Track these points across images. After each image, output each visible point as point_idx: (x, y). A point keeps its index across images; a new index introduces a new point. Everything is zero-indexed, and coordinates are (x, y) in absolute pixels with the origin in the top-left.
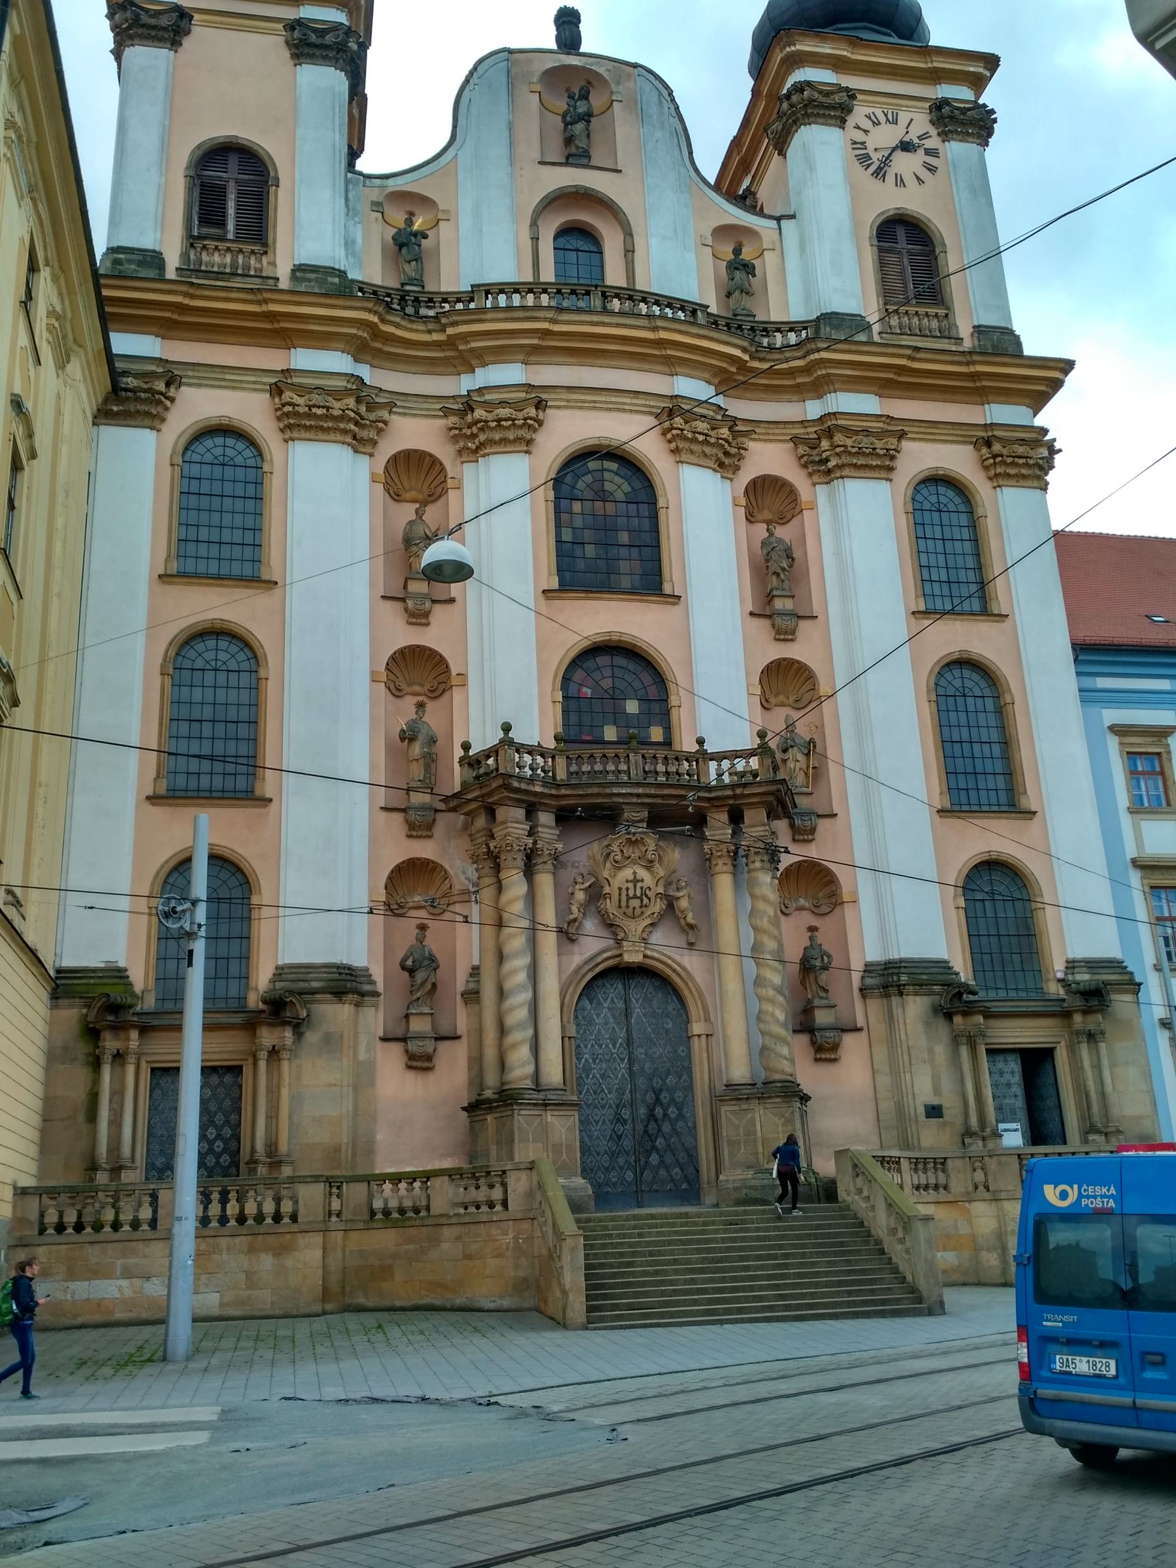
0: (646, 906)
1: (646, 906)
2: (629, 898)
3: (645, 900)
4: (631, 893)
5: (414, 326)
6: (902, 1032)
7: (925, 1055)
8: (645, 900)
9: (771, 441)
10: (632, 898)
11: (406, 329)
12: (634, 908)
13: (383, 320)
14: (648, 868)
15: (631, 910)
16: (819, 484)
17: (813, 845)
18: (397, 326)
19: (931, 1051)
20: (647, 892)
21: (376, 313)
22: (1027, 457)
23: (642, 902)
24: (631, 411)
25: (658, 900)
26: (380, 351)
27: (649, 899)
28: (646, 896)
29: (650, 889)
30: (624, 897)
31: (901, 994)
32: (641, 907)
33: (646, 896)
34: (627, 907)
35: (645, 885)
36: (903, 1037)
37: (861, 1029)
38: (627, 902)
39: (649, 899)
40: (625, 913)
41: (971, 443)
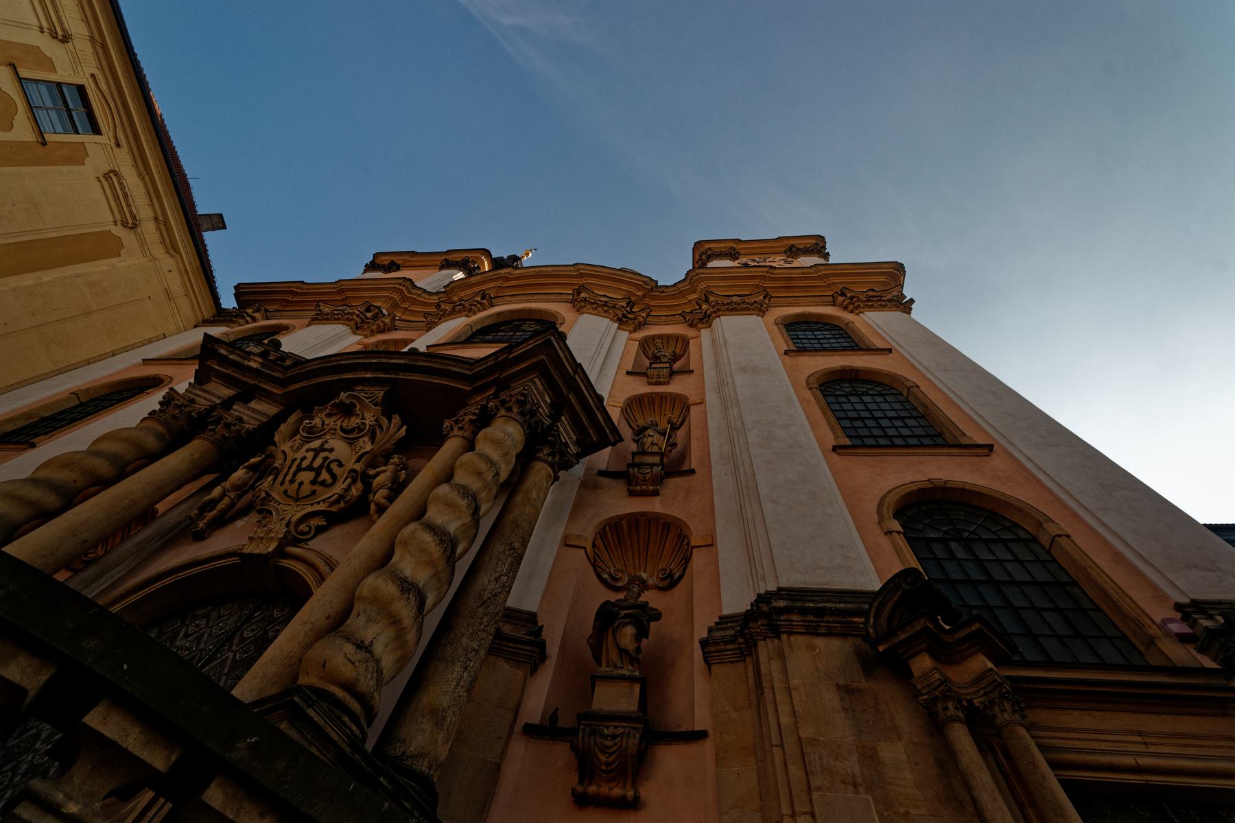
0: (323, 483)
1: (323, 483)
2: (299, 469)
3: (325, 475)
4: (305, 464)
5: (431, 297)
6: (784, 709)
7: (852, 765)
8: (325, 475)
9: (669, 324)
10: (304, 469)
11: (425, 298)
12: (301, 483)
13: (409, 292)
14: (351, 442)
15: (296, 485)
16: (702, 328)
17: (658, 499)
18: (419, 296)
19: (869, 756)
20: (334, 466)
21: (404, 286)
22: (880, 297)
23: (318, 474)
24: (554, 302)
25: (349, 480)
26: (406, 309)
27: (334, 477)
28: (330, 471)
29: (340, 465)
30: (294, 468)
31: (776, 632)
32: (313, 482)
33: (330, 471)
34: (292, 481)
35: (332, 456)
36: (785, 720)
37: (702, 735)
38: (295, 474)
39: (334, 477)
40: (285, 492)
41: (832, 305)
